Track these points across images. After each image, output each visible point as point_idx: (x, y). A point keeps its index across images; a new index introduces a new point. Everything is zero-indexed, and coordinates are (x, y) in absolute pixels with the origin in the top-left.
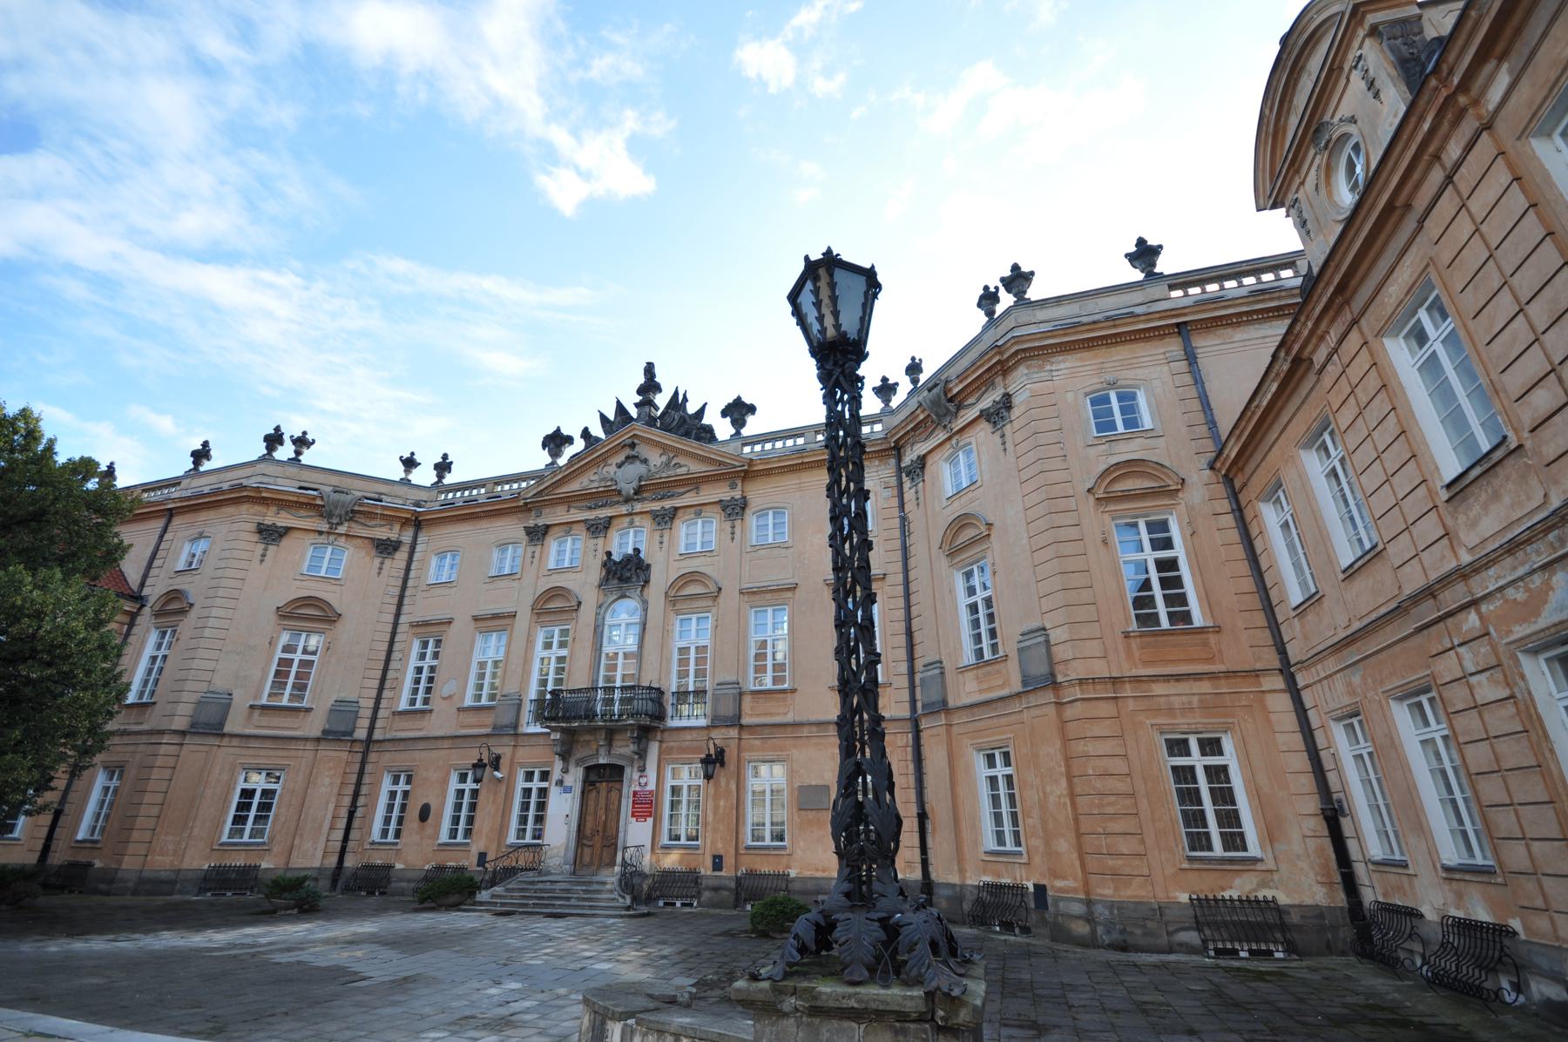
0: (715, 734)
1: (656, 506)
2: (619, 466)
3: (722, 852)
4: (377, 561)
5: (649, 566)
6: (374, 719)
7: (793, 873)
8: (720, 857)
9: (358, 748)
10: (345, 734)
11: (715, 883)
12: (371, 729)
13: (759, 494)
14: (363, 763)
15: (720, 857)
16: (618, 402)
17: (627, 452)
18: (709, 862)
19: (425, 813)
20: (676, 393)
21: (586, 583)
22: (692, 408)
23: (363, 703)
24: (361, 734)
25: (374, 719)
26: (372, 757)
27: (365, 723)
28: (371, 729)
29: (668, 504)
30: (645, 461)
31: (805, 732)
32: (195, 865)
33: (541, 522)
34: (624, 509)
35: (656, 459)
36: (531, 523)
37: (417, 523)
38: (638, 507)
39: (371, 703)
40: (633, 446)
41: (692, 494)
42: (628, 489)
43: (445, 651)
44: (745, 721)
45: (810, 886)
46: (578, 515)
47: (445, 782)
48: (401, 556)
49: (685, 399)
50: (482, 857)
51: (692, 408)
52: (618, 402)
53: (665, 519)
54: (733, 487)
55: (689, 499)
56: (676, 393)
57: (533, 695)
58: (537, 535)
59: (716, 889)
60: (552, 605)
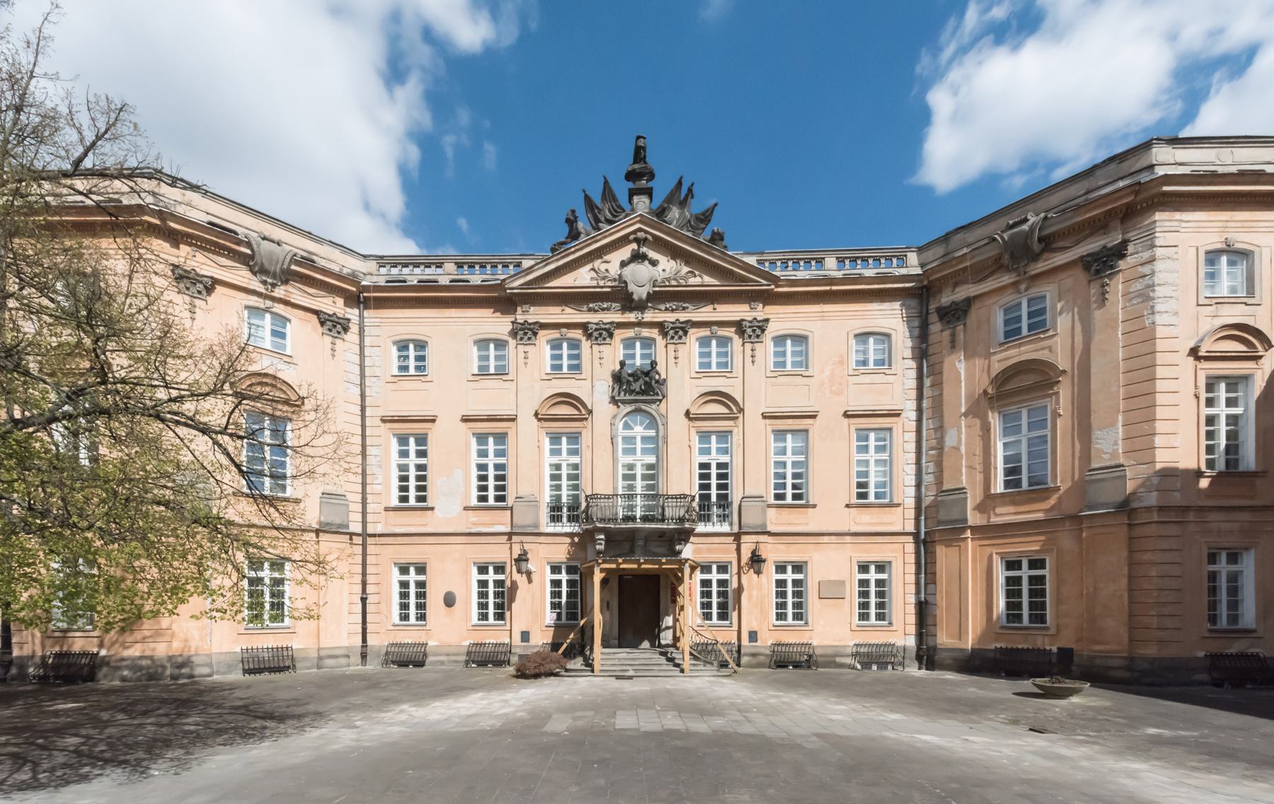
1: (670, 317)
2: (623, 264)
3: (755, 629)
4: (328, 339)
6: (364, 513)
7: (815, 643)
8: (755, 633)
9: (358, 540)
10: (340, 526)
11: (753, 651)
12: (364, 523)
13: (782, 319)
14: (364, 555)
15: (755, 633)
18: (745, 636)
19: (449, 601)
20: (680, 183)
21: (595, 387)
23: (350, 497)
24: (356, 527)
25: (364, 513)
26: (370, 549)
27: (359, 517)
28: (364, 523)
29: (683, 317)
30: (654, 263)
31: (826, 539)
32: (225, 649)
33: (531, 319)
34: (631, 317)
36: (520, 318)
37: (360, 298)
38: (649, 316)
39: (359, 498)
41: (710, 308)
43: (431, 448)
44: (770, 528)
45: (830, 651)
47: (467, 573)
48: (352, 336)
50: (525, 636)
52: (606, 182)
53: (679, 331)
55: (705, 313)
56: (680, 183)
57: (547, 496)
58: (525, 332)
59: (754, 655)
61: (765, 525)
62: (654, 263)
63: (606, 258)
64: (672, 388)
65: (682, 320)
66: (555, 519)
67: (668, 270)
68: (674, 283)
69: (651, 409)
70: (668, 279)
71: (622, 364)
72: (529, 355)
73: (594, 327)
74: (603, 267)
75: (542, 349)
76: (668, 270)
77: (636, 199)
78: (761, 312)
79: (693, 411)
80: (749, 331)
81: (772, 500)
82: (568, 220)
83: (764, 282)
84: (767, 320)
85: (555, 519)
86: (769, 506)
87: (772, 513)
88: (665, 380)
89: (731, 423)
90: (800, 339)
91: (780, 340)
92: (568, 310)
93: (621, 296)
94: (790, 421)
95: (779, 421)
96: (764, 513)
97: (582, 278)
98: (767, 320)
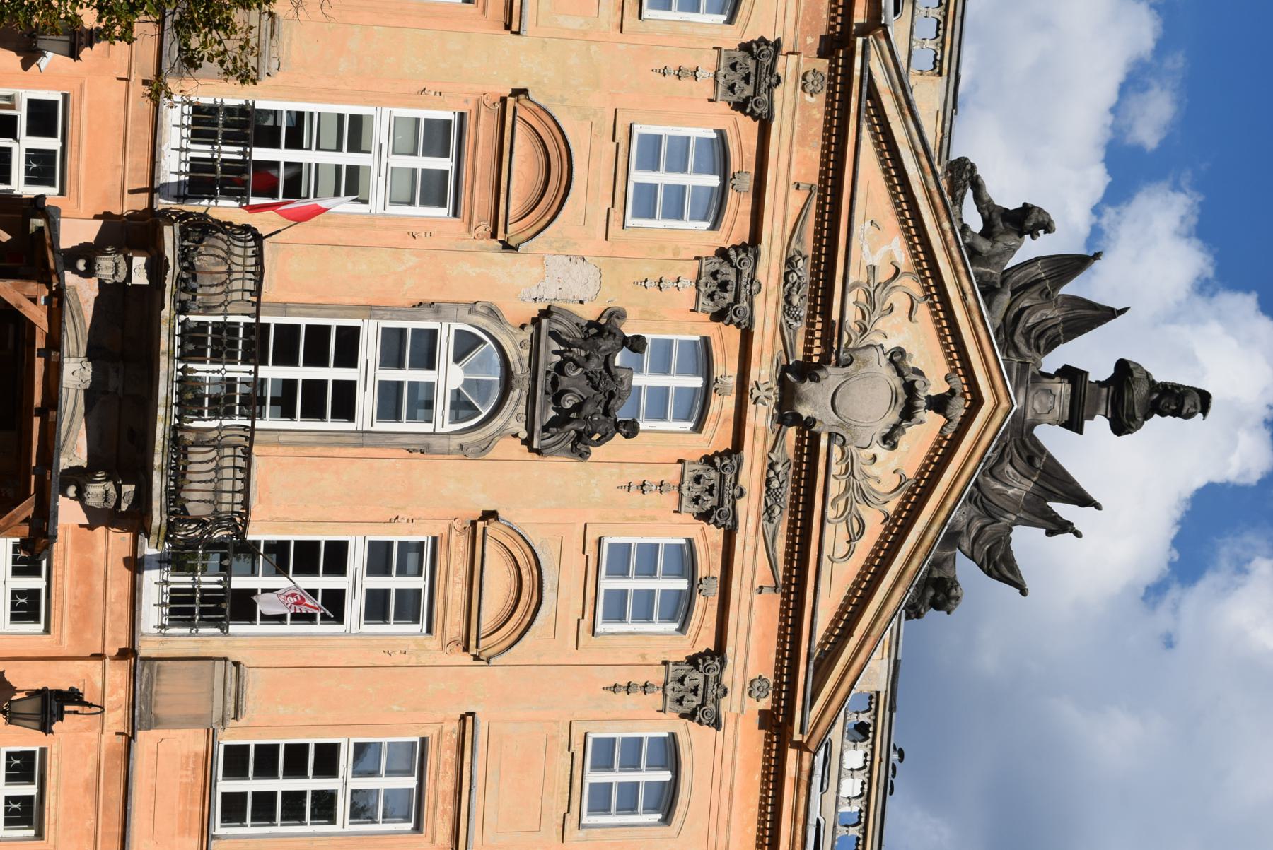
0: (118, 674)
1: (751, 474)
2: (897, 359)
5: (583, 456)
16: (1110, 314)
17: (936, 378)
20: (1084, 500)
22: (1027, 542)
29: (749, 510)
34: (763, 372)
35: (891, 468)
38: (760, 416)
40: (939, 404)
41: (763, 574)
42: (814, 402)
44: (145, 739)
46: (787, 204)
49: (1059, 527)
51: (1027, 542)
52: (1110, 314)
54: (753, 688)
56: (1084, 500)
60: (523, 146)
61: (154, 722)
62: (889, 439)
63: (923, 310)
64: (560, 470)
65: (741, 504)
66: (205, 122)
67: (874, 470)
68: (835, 488)
69: (512, 418)
70: (849, 471)
71: (636, 344)
72: (687, 82)
73: (746, 270)
74: (899, 300)
75: (702, 118)
76: (874, 470)
77: (1062, 388)
78: (742, 710)
79: (493, 528)
80: (699, 678)
81: (229, 737)
82: (1026, 209)
83: (812, 715)
84: (717, 724)
85: (205, 122)
86: (211, 736)
87: (194, 741)
88: (583, 456)
89: (455, 629)
90: (666, 801)
91: (669, 753)
92: (797, 200)
93: (823, 348)
94: (447, 785)
95: (449, 756)
96: (191, 722)
97: (875, 243)
98: (717, 724)
